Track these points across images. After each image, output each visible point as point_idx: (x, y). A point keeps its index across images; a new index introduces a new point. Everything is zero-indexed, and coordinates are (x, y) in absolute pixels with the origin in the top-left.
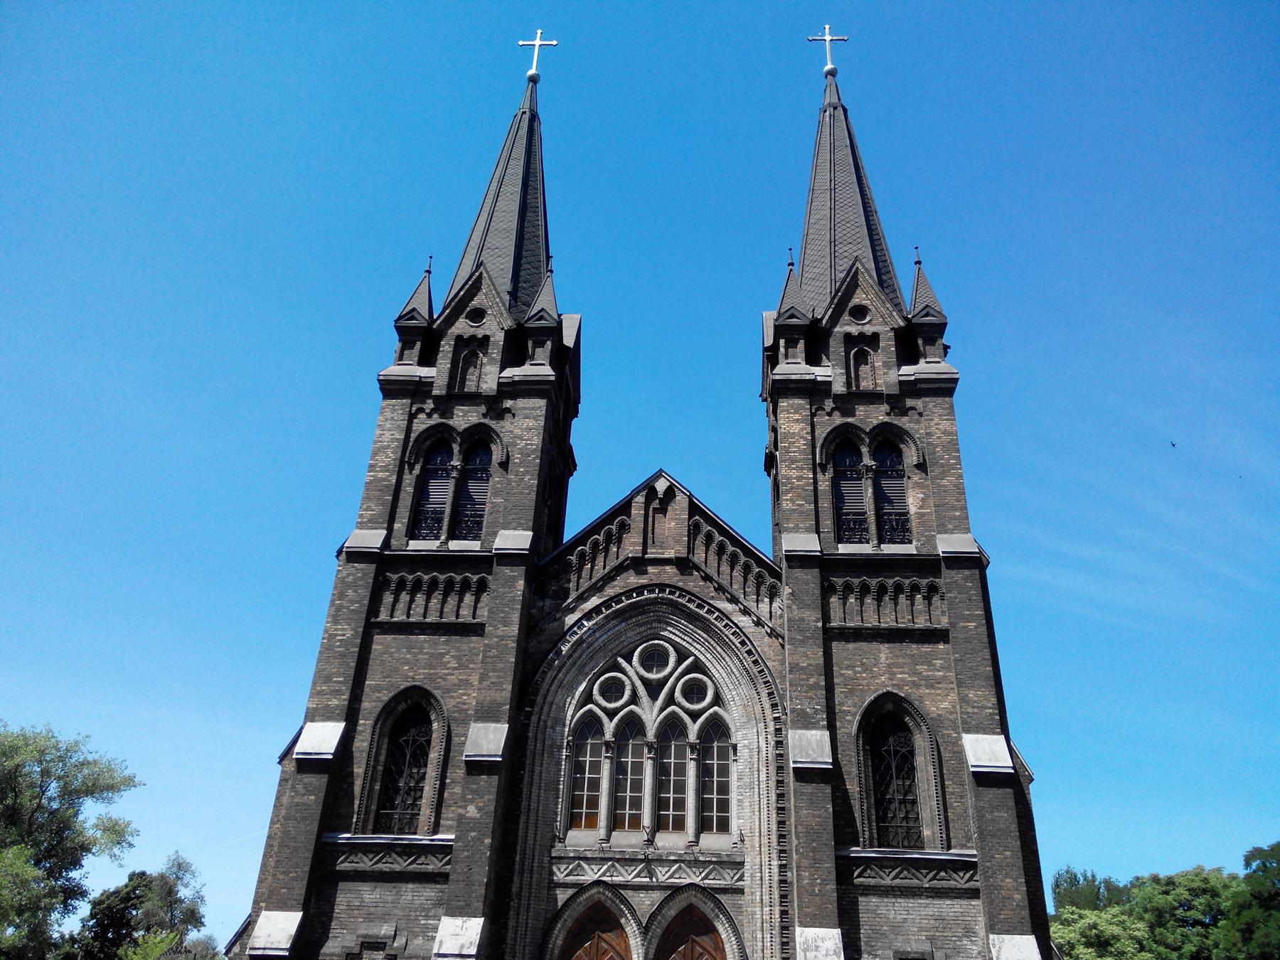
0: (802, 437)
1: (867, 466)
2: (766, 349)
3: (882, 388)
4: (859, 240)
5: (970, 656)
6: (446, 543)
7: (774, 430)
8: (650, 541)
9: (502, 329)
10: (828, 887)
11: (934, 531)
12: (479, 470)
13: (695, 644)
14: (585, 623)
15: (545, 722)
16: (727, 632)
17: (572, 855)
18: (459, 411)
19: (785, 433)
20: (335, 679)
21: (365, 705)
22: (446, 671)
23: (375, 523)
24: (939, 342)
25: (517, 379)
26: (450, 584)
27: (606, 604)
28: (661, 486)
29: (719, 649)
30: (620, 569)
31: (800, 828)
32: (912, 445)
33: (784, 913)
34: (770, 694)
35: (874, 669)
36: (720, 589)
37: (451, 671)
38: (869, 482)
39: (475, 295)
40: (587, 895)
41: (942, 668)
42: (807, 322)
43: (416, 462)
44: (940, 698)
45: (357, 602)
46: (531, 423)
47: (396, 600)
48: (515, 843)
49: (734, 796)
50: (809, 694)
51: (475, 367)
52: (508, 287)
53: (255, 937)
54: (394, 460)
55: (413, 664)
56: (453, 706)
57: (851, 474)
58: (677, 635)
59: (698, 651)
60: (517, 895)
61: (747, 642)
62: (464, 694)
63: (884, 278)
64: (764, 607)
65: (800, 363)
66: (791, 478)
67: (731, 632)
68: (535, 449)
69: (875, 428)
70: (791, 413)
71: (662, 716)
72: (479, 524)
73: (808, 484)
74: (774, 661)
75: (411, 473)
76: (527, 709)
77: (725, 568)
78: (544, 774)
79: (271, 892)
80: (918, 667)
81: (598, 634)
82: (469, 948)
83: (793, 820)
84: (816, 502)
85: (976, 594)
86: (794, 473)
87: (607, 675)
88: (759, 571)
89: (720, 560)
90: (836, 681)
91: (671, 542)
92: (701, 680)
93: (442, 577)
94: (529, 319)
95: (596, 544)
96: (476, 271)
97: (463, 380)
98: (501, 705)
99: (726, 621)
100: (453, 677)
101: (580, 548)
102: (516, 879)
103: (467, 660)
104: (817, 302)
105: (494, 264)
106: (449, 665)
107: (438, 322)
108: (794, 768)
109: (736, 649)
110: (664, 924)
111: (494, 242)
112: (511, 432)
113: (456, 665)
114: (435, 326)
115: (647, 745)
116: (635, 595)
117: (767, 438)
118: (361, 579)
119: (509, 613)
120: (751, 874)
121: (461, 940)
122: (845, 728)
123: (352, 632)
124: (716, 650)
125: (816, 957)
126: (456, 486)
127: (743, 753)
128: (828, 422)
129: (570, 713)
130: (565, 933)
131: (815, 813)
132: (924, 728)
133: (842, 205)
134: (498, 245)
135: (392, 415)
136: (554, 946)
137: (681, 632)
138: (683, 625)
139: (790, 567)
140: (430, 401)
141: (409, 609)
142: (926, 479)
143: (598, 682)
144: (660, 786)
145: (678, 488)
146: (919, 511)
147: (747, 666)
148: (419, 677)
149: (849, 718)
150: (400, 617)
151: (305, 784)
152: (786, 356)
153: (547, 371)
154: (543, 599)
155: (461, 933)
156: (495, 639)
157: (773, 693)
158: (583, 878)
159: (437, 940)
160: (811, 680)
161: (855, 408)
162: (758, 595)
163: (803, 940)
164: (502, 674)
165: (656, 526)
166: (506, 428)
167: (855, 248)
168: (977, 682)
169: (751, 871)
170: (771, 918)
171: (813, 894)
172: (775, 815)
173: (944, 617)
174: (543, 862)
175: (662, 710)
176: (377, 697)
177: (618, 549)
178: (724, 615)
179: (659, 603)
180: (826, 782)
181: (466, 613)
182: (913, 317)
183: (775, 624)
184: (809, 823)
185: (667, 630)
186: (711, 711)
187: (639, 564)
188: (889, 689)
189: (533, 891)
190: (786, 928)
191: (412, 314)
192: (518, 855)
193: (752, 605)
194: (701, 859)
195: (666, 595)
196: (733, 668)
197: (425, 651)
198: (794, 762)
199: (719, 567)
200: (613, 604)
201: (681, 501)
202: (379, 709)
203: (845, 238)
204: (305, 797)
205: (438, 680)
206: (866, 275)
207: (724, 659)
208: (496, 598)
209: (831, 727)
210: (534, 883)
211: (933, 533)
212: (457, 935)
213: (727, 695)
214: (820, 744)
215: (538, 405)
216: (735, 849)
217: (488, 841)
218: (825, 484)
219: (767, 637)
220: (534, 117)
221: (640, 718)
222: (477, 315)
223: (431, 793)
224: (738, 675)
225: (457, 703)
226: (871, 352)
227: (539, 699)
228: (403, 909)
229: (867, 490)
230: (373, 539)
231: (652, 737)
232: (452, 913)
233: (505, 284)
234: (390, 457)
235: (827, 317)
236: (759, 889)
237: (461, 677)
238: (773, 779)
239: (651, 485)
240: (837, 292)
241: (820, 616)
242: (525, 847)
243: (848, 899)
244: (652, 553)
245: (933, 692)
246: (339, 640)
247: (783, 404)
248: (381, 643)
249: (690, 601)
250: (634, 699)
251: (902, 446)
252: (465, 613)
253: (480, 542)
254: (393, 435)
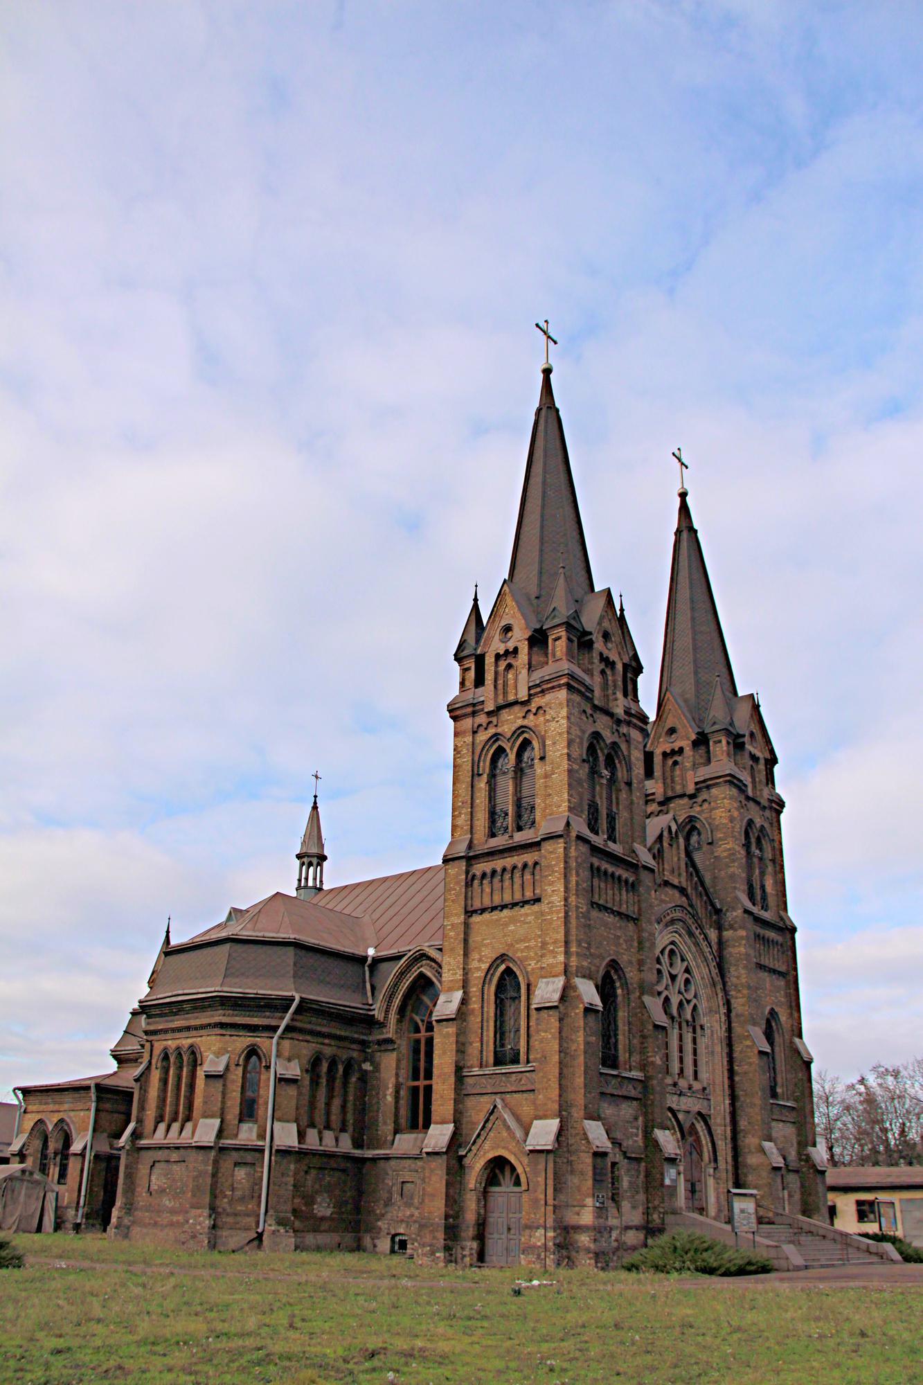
9: (622, 659)
86: (736, 847)
127: (708, 1032)
213: (701, 992)
246: (582, 913)
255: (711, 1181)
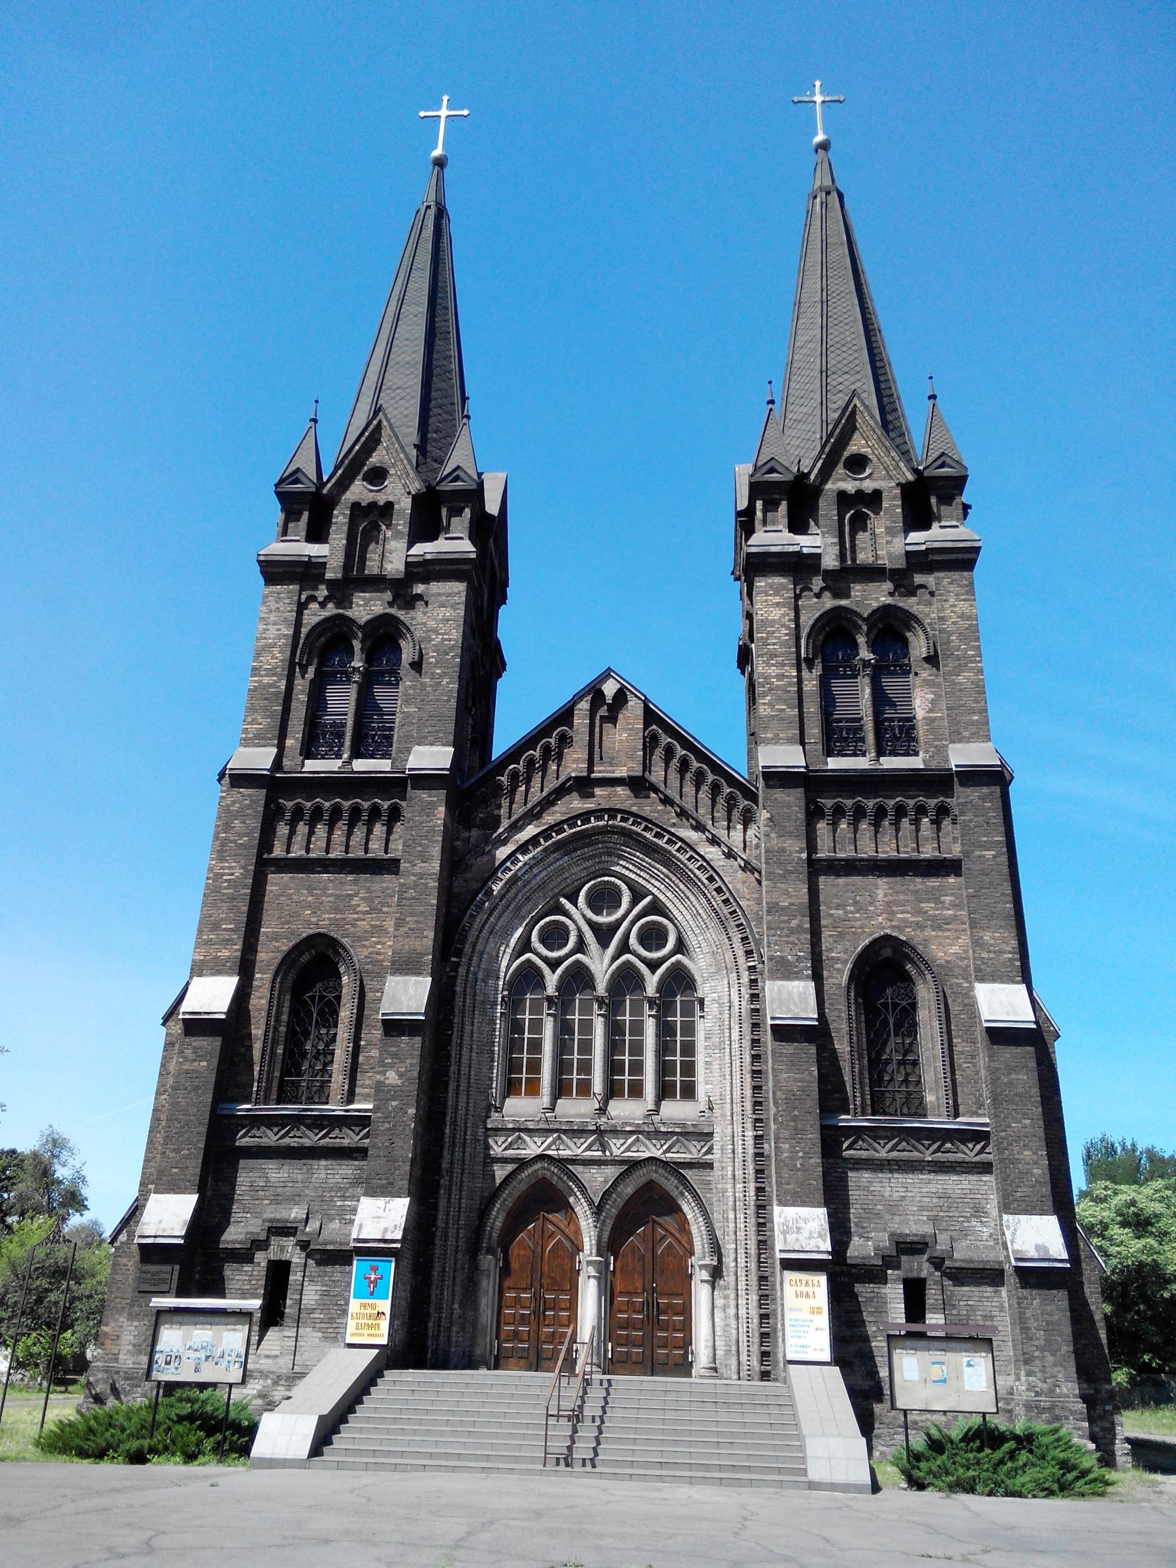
0: (782, 626)
1: (863, 660)
2: (739, 514)
3: (884, 562)
4: (858, 369)
5: (986, 890)
6: (349, 762)
7: (749, 616)
8: (597, 757)
9: (409, 493)
10: (812, 1161)
11: (946, 740)
12: (387, 672)
13: (653, 881)
14: (520, 857)
15: (475, 974)
16: (691, 866)
17: (510, 1126)
18: (359, 598)
19: (762, 620)
20: (224, 926)
21: (262, 956)
22: (356, 916)
23: (262, 738)
24: (958, 500)
25: (428, 557)
26: (356, 812)
27: (545, 834)
28: (610, 689)
29: (682, 886)
30: (561, 792)
31: (779, 1093)
32: (921, 633)
33: (760, 1190)
34: (744, 939)
35: (870, 908)
36: (683, 814)
37: (361, 916)
38: (867, 680)
39: (374, 450)
40: (530, 1170)
41: (953, 905)
42: (790, 478)
43: (309, 663)
44: (948, 941)
45: (245, 835)
46: (448, 612)
47: (292, 833)
48: (444, 1114)
49: (700, 1058)
50: (791, 939)
51: (377, 543)
52: (414, 438)
53: (144, 1224)
54: (282, 661)
55: (316, 909)
56: (366, 957)
57: (845, 671)
58: (631, 870)
59: (657, 889)
60: (447, 1171)
61: (716, 877)
62: (378, 943)
63: (890, 418)
64: (737, 835)
65: (781, 531)
66: (770, 677)
67: (697, 866)
68: (454, 646)
69: (874, 612)
70: (770, 595)
71: (614, 966)
72: (389, 739)
73: (790, 684)
74: (748, 900)
75: (303, 677)
76: (453, 959)
77: (689, 789)
78: (475, 1035)
79: (161, 1172)
80: (922, 905)
81: (535, 871)
82: (393, 1232)
83: (771, 1084)
84: (800, 706)
85: (996, 817)
86: (773, 671)
87: (548, 919)
88: (731, 792)
89: (682, 779)
90: (823, 922)
91: (622, 757)
92: (660, 924)
93: (346, 804)
94: (442, 480)
95: (531, 762)
96: (374, 418)
97: (363, 560)
98: (422, 955)
99: (691, 853)
100: (364, 923)
101: (512, 766)
102: (446, 1153)
103: (379, 903)
104: (804, 451)
105: (396, 409)
106: (359, 909)
107: (329, 485)
108: (771, 1025)
109: (702, 887)
110: (620, 1202)
111: (395, 381)
112: (425, 624)
113: (368, 909)
114: (325, 491)
115: (597, 1001)
116: (579, 823)
117: (741, 626)
118: (249, 807)
119: (428, 846)
120: (722, 1146)
121: (384, 1223)
122: (832, 977)
123: (242, 871)
124: (678, 887)
125: (797, 1240)
126: (359, 693)
127: (711, 1008)
128: (815, 607)
129: (504, 964)
130: (505, 1214)
131: (797, 1076)
132: (929, 977)
133: (836, 322)
134: (400, 383)
135: (277, 605)
136: (492, 1228)
137: (636, 866)
138: (638, 858)
139: (768, 786)
140: (323, 587)
141: (309, 842)
142: (937, 675)
143: (537, 927)
144: (613, 1047)
145: (630, 691)
146: (927, 715)
147: (716, 906)
148: (324, 923)
149: (839, 966)
150: (297, 852)
151: (195, 1048)
152: (765, 523)
153: (465, 547)
154: (469, 829)
155: (384, 1215)
156: (412, 878)
157: (747, 938)
158: (524, 1152)
159: (356, 1223)
160: (793, 922)
161: (849, 588)
162: (729, 821)
163: (782, 1220)
164: (421, 919)
165: (604, 738)
166: (419, 620)
167: (852, 380)
168: (993, 922)
169: (721, 1143)
170: (745, 1196)
171: (794, 1169)
172: (749, 1080)
173: (956, 845)
174: (477, 1134)
175: (614, 959)
176: (275, 947)
177: (558, 766)
178: (687, 845)
179: (609, 832)
180: (809, 1041)
181: (376, 847)
182: (925, 469)
183: (751, 855)
184: (790, 1088)
185: (619, 864)
186: (673, 959)
187: (584, 785)
188: (888, 931)
189: (466, 1167)
190: (762, 1208)
191: (295, 476)
192: (448, 1127)
193: (721, 833)
194: (663, 1129)
195: (617, 822)
196: (699, 908)
197: (329, 892)
198: (772, 1018)
199: (681, 787)
200: (554, 834)
201: (634, 707)
202: (278, 961)
203: (840, 366)
204: (196, 1064)
205: (346, 926)
206: (866, 414)
207: (688, 898)
208: (411, 828)
209: (817, 977)
210: (467, 1158)
211: (945, 743)
212: (379, 1217)
213: (692, 940)
214: (803, 997)
215: (456, 590)
216: (703, 1118)
217: (412, 1111)
218: (811, 684)
219: (740, 872)
220: (441, 213)
221: (587, 969)
222: (378, 476)
223: (344, 1058)
224: (705, 917)
225: (370, 953)
226: (872, 515)
227: (468, 948)
228: (315, 1189)
229: (863, 691)
230: (261, 759)
231: (603, 991)
232: (372, 1193)
233: (410, 433)
234: (277, 658)
235: (816, 471)
236: (731, 1164)
237: (373, 923)
238: (748, 1037)
239: (597, 687)
240: (829, 436)
241: (805, 845)
242: (456, 1117)
243: (836, 1174)
244: (600, 772)
245: (941, 934)
246: (226, 881)
247: (760, 583)
248: (276, 882)
249: (646, 829)
250: (581, 947)
251: (908, 634)
252: (374, 847)
253: (390, 761)
254: (279, 630)
255: (701, 1294)
